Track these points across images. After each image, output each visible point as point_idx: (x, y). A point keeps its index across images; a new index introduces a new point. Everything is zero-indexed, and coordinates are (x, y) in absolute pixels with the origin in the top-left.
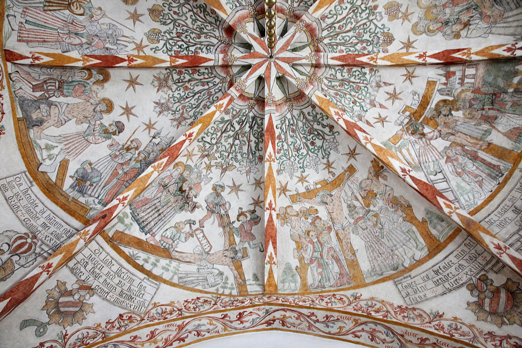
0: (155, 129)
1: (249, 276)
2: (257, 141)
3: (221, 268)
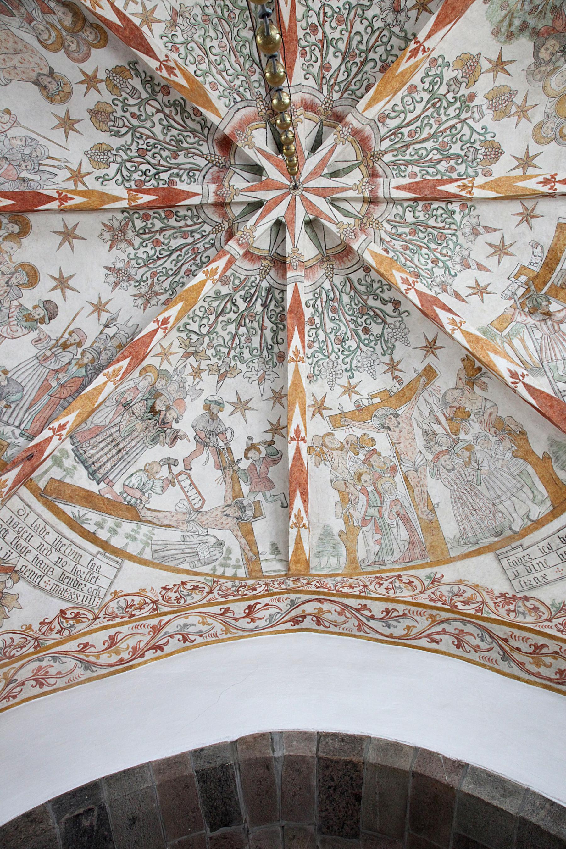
0: (107, 311)
1: (264, 546)
2: (275, 329)
3: (220, 534)
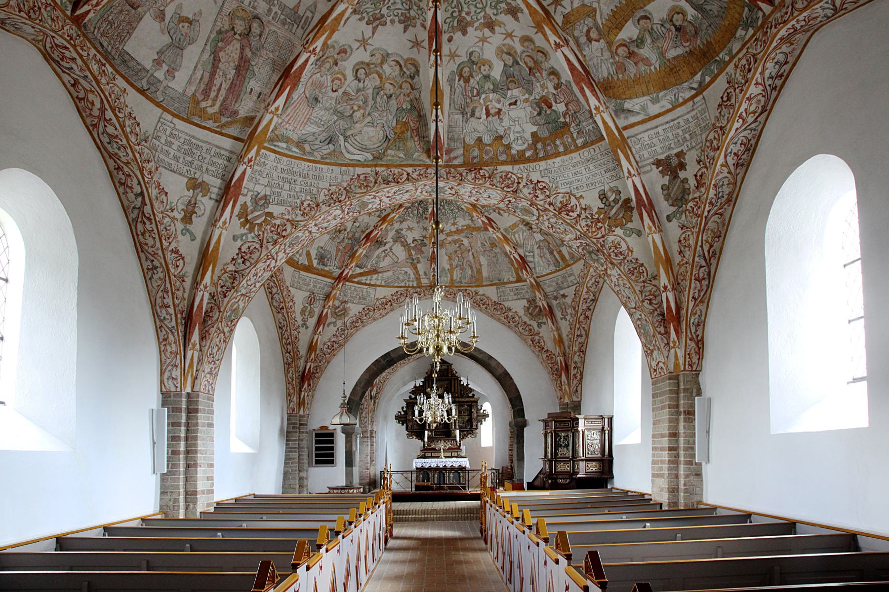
3: (405, 269)
